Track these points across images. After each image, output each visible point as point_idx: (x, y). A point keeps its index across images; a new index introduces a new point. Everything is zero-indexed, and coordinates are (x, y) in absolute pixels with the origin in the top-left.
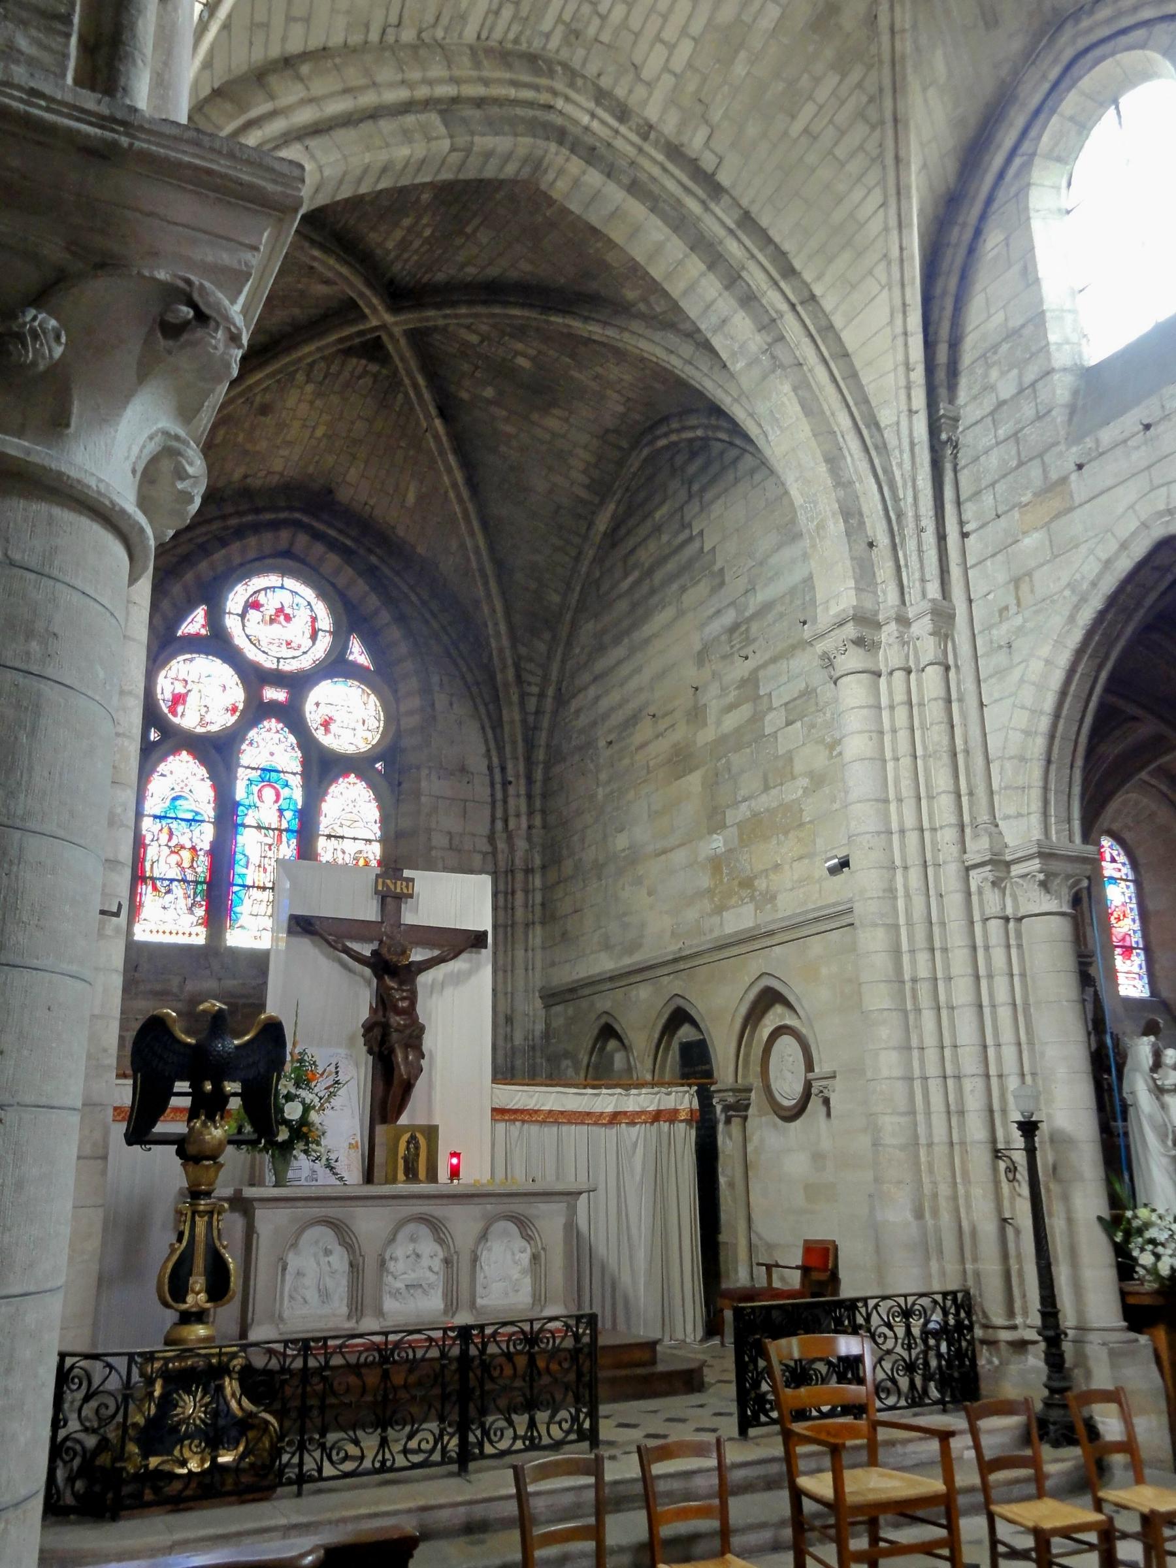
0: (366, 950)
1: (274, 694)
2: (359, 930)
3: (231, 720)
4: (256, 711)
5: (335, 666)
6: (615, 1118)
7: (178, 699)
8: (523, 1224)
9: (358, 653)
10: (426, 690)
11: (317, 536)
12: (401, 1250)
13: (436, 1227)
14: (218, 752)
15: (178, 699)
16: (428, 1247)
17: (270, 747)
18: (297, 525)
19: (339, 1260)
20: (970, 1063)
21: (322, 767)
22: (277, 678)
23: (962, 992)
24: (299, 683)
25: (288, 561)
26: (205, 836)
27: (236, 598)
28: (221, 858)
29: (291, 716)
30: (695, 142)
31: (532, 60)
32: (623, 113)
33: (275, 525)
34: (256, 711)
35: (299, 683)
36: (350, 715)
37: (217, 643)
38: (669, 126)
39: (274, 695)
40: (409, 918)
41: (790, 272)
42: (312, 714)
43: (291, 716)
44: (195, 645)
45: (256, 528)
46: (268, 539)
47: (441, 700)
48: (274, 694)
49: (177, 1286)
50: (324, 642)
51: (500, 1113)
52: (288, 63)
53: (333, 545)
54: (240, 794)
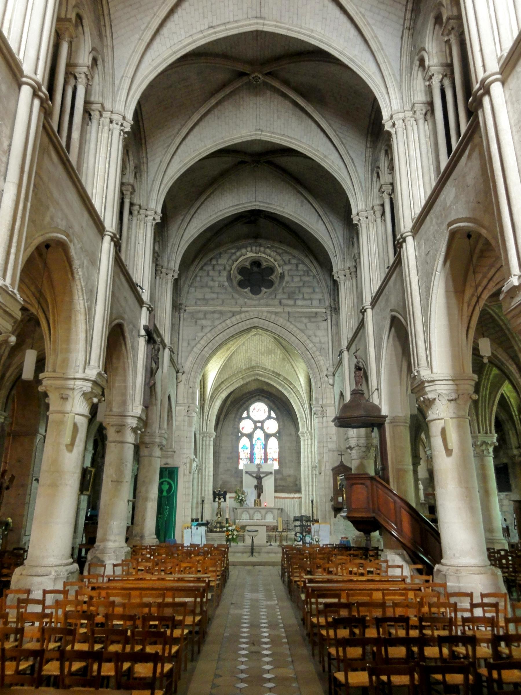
0: (255, 475)
1: (259, 425)
2: (254, 472)
3: (252, 430)
4: (256, 428)
5: (269, 417)
6: (293, 498)
7: (243, 428)
8: (272, 512)
9: (273, 415)
10: (283, 421)
11: (263, 396)
12: (256, 515)
13: (260, 512)
14: (250, 436)
15: (243, 428)
16: (259, 515)
17: (259, 434)
18: (259, 395)
19: (248, 515)
20: (311, 493)
21: (267, 436)
22: (259, 422)
23: (310, 484)
24: (262, 422)
25: (259, 400)
26: (249, 451)
27: (251, 408)
28: (252, 454)
29: (262, 428)
30: (276, 370)
31: (253, 367)
32: (266, 369)
33: (255, 396)
34: (256, 428)
35: (262, 422)
36: (272, 426)
37: (249, 417)
38: (272, 369)
39: (259, 425)
40: (262, 470)
41: (291, 384)
42: (265, 426)
43: (262, 428)
44: (245, 418)
45: (252, 397)
46: (255, 398)
47: (286, 422)
48: (259, 425)
49: (217, 515)
50: (267, 414)
51: (276, 497)
52: (222, 382)
53: (266, 398)
54: (254, 443)
